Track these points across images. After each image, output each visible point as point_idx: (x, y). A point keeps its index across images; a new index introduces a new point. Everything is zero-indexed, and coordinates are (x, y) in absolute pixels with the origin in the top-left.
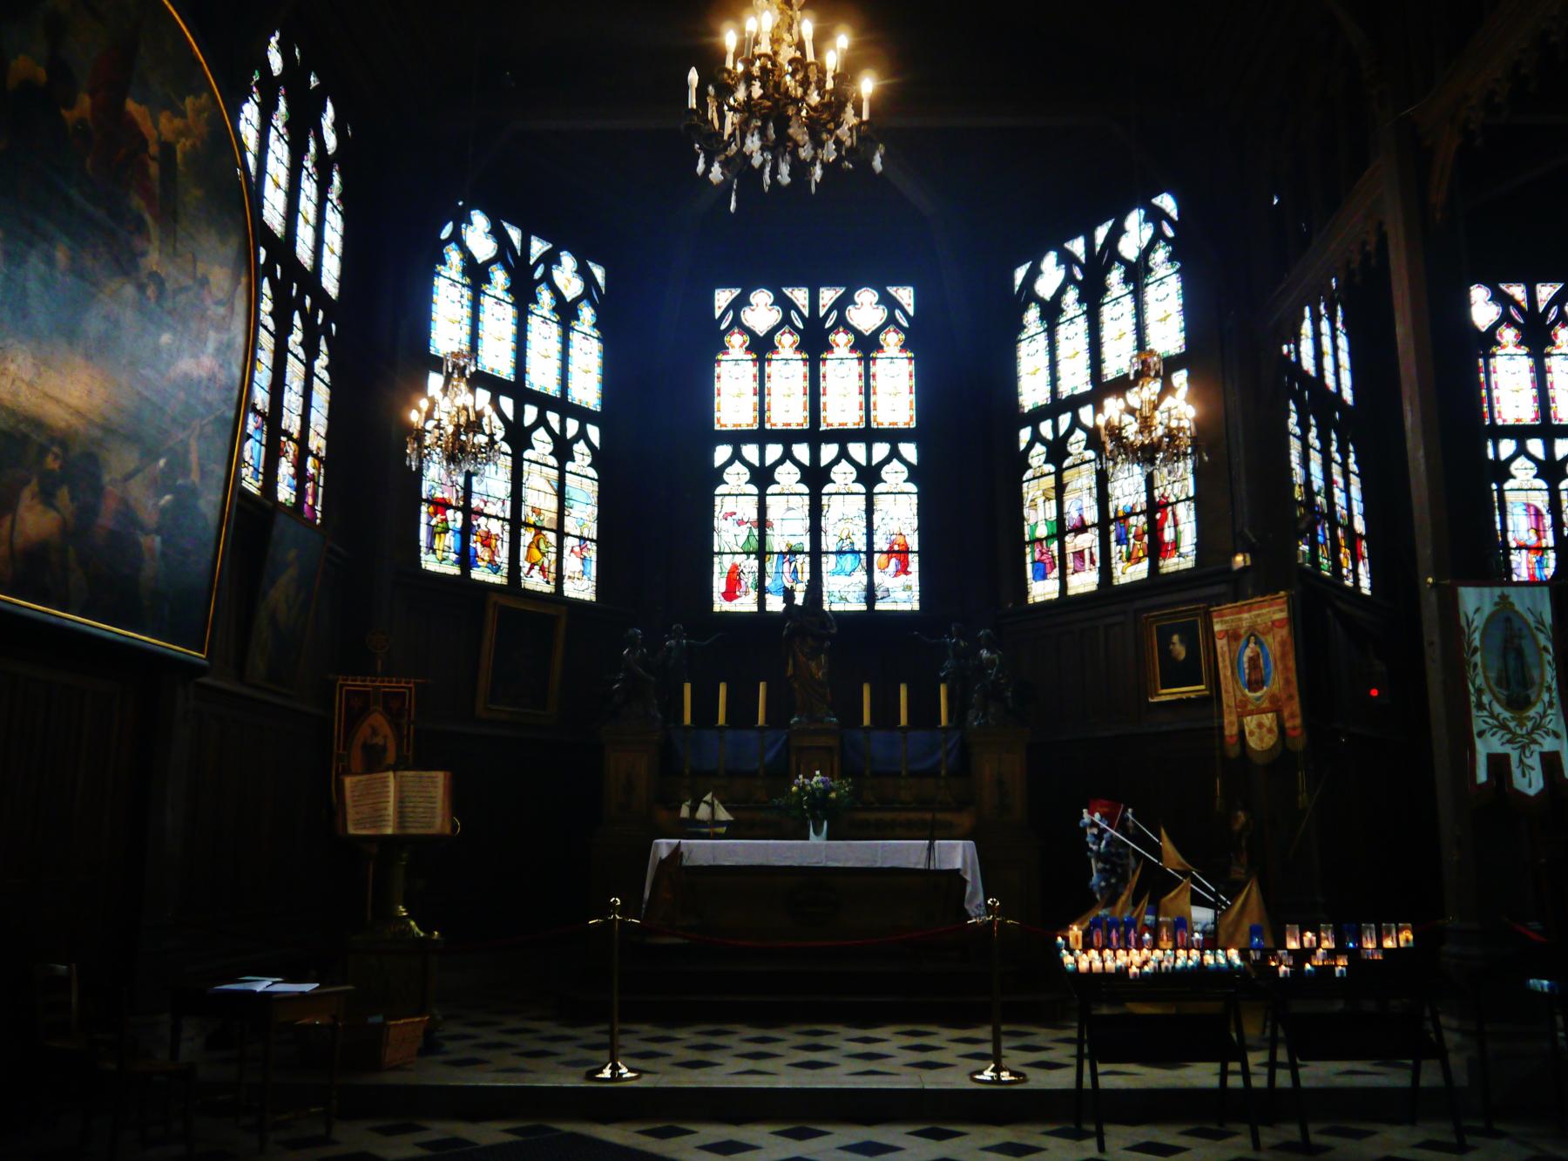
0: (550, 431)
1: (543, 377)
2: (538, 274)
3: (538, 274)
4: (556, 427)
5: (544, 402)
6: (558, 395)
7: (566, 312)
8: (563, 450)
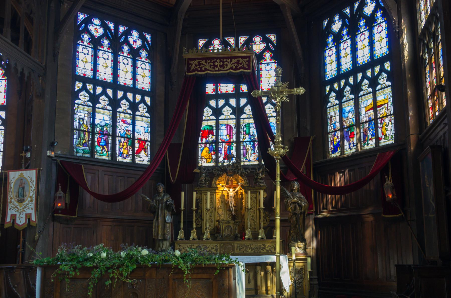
0: (128, 100)
1: (125, 78)
2: (122, 40)
3: (122, 40)
4: (131, 100)
5: (125, 89)
6: (132, 86)
7: (134, 54)
8: (134, 107)
